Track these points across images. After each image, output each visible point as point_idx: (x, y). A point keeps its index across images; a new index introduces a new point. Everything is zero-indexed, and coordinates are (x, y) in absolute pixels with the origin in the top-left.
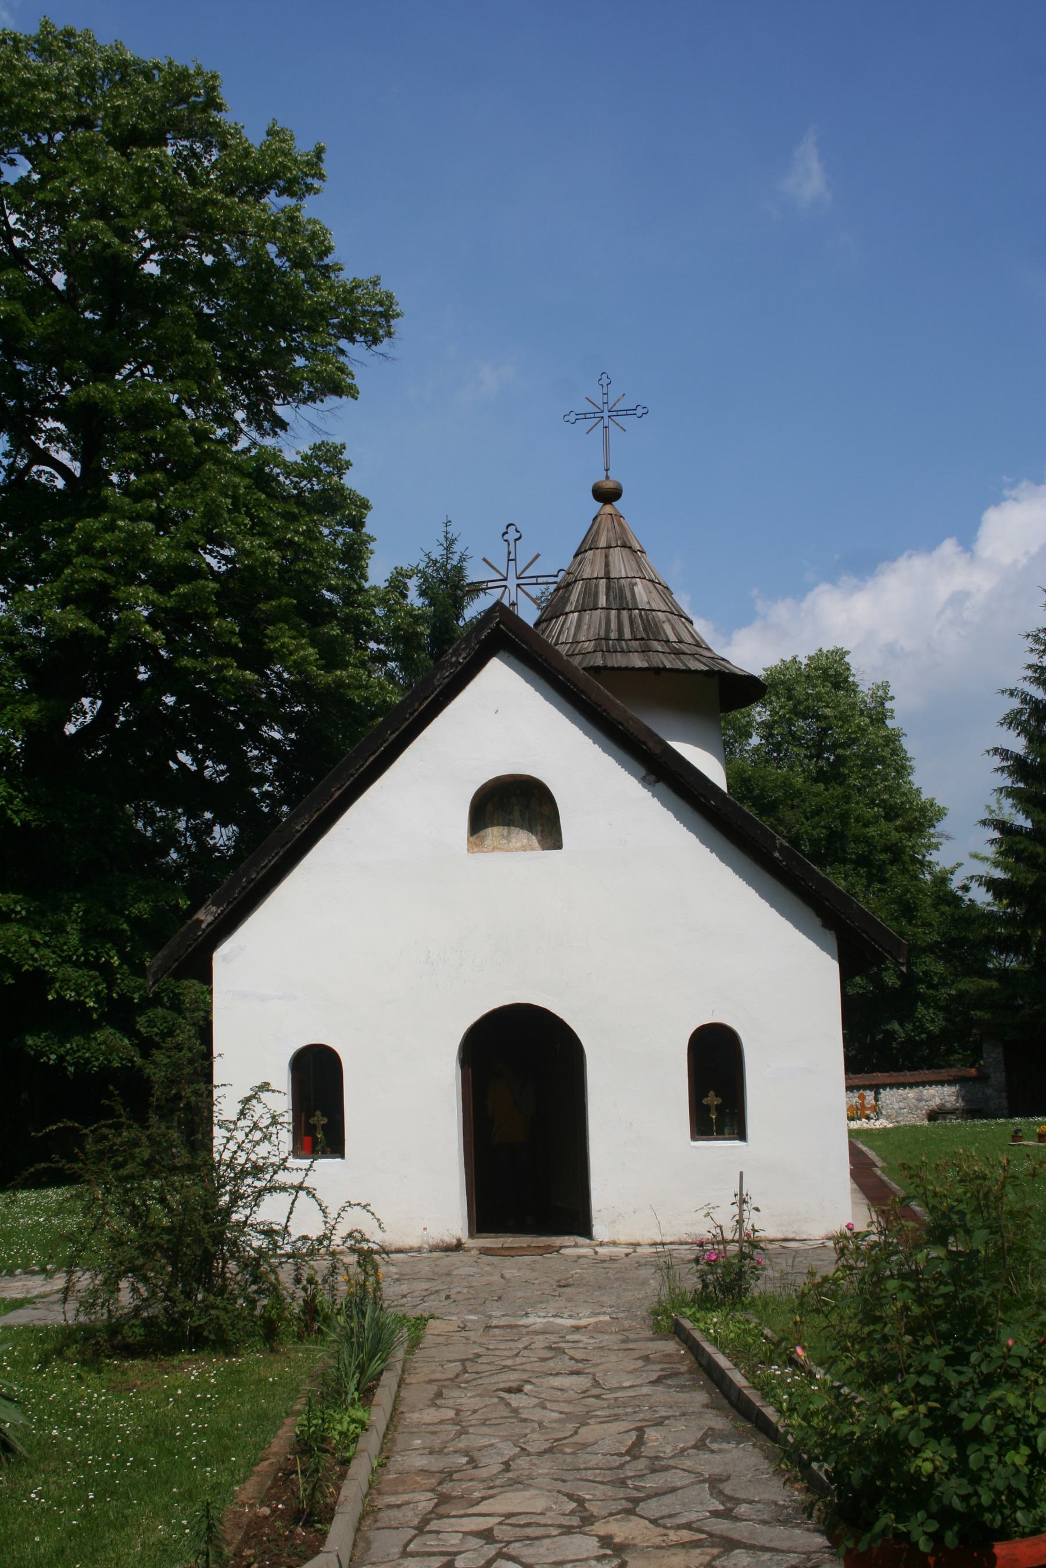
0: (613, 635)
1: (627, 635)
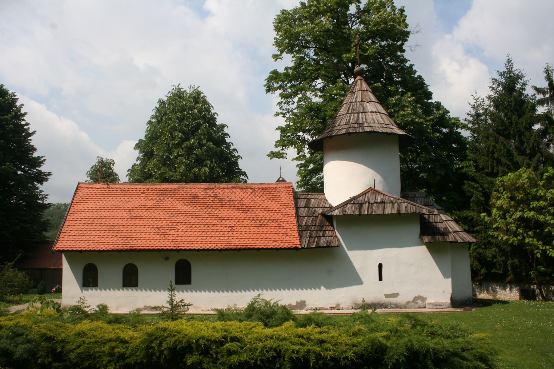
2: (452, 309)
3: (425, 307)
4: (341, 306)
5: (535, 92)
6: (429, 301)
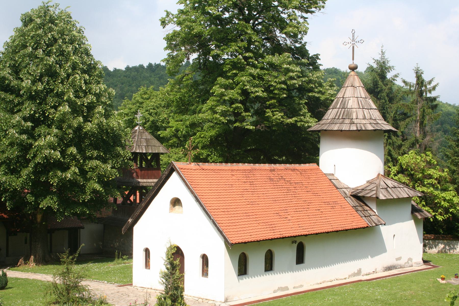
0: (337, 118)
1: (341, 118)
2: (425, 267)
4: (377, 270)
5: (402, 84)
6: (414, 261)
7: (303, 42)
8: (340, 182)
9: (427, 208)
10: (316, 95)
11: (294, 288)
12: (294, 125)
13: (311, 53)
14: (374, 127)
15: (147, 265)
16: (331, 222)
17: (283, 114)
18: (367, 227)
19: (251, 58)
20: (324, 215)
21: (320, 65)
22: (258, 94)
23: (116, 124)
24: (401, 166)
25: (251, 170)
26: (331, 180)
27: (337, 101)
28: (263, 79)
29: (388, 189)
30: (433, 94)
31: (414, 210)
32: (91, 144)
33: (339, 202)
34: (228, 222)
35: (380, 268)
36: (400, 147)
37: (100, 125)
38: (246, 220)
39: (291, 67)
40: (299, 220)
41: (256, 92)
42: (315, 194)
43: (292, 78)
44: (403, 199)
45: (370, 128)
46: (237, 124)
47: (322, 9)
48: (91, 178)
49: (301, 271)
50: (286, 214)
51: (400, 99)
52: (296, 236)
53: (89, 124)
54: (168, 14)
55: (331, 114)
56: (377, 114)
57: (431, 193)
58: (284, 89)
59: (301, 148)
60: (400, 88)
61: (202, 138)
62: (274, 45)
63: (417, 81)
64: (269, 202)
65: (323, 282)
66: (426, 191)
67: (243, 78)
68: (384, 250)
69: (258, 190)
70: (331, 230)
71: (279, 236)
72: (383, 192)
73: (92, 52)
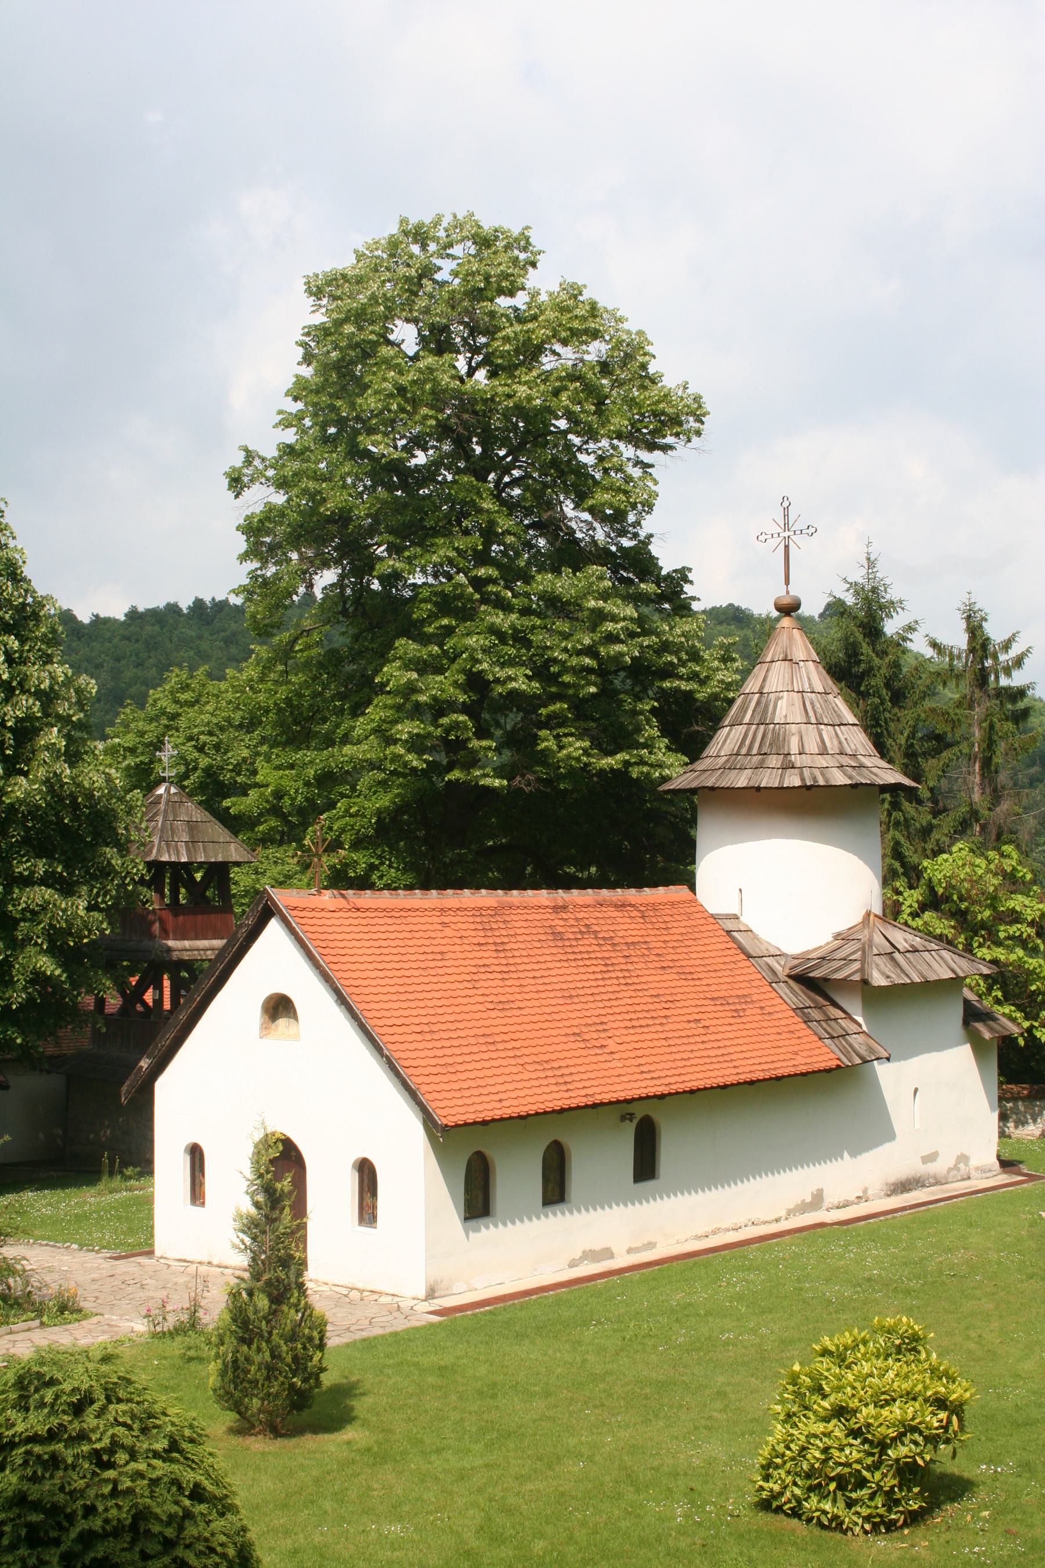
0: (744, 751)
1: (755, 751)
2: (1004, 1178)
3: (969, 1178)
4: (870, 1192)
5: (929, 653)
6: (974, 1162)
7: (643, 534)
8: (756, 937)
9: (1007, 1009)
10: (684, 686)
11: (629, 1251)
12: (620, 776)
13: (667, 565)
14: (850, 778)
15: (197, 1194)
16: (733, 1057)
17: (587, 744)
18: (838, 1066)
19: (490, 580)
20: (713, 1037)
21: (693, 598)
22: (514, 684)
23: (100, 781)
24: (931, 889)
25: (497, 910)
26: (730, 934)
27: (744, 703)
28: (527, 644)
29: (897, 955)
30: (1017, 679)
31: (972, 1015)
32: (26, 841)
33: (755, 998)
34: (433, 1062)
35: (876, 1186)
36: (926, 832)
37: (52, 784)
38: (486, 1056)
39: (609, 607)
40: (639, 1053)
41: (510, 679)
42: (685, 975)
43: (612, 638)
44: (940, 983)
45: (839, 779)
46: (455, 775)
47: (694, 439)
48: (28, 940)
49: (648, 1201)
50: (603, 1035)
51: (924, 695)
52: (633, 1100)
53: (22, 780)
54: (250, 456)
55: (726, 741)
56: (858, 740)
57: (1020, 964)
58: (589, 670)
59: (643, 842)
60: (922, 663)
61: (351, 816)
62: (558, 544)
63: (969, 643)
64: (553, 1002)
65: (714, 1233)
66: (1003, 958)
67: (471, 641)
68: (889, 1135)
69: (521, 968)
70: (733, 1079)
71: (582, 1101)
72: (882, 967)
73: (27, 571)
